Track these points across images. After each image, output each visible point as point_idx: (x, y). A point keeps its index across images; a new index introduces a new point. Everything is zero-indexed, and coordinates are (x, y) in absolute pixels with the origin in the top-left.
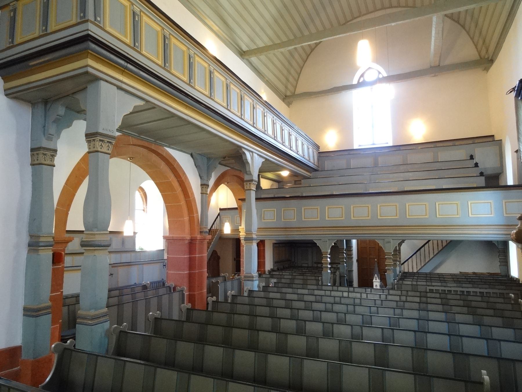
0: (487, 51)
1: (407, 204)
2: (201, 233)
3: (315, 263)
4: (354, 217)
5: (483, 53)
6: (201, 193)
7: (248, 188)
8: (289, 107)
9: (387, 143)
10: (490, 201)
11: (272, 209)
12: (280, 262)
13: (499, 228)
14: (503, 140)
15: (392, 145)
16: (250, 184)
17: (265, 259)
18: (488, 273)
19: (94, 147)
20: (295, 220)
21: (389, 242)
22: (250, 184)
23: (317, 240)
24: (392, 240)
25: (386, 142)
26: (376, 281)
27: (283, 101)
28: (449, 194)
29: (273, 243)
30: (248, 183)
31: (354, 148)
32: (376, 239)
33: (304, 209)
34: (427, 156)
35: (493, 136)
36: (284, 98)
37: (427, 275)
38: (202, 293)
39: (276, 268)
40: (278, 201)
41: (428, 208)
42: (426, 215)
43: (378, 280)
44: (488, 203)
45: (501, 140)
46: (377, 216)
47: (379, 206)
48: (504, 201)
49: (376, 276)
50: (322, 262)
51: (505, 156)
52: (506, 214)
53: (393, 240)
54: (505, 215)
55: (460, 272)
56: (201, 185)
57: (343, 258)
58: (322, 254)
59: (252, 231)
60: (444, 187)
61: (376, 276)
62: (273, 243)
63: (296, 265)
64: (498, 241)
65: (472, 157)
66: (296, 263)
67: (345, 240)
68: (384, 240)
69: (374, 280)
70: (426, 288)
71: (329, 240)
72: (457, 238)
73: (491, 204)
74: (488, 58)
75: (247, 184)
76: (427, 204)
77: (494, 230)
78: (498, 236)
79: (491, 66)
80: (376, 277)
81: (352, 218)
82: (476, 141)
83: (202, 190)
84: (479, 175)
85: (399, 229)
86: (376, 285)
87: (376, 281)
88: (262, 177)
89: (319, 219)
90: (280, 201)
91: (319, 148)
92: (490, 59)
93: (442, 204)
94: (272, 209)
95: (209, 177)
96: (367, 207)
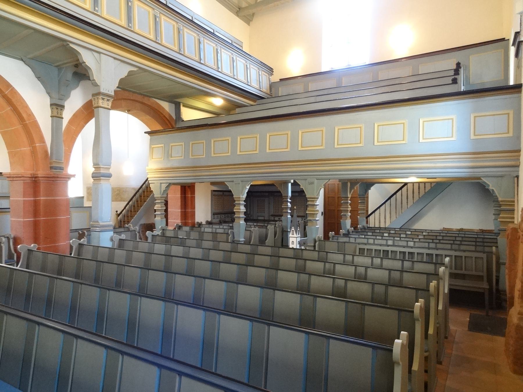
1: (336, 128)
2: (51, 169)
3: (272, 215)
6: (51, 117)
8: (249, 24)
12: (224, 214)
13: (466, 158)
16: (97, 98)
17: (194, 208)
18: (481, 230)
20: (204, 156)
21: (312, 183)
23: (228, 182)
24: (316, 181)
27: (238, 16)
29: (211, 190)
31: (322, 71)
32: (297, 180)
36: (238, 11)
37: (395, 231)
38: (55, 246)
39: (216, 221)
41: (363, 133)
42: (360, 143)
44: (448, 119)
49: (293, 227)
50: (234, 210)
51: (510, 60)
52: (475, 135)
53: (317, 179)
54: (473, 137)
56: (51, 105)
57: (287, 208)
58: (235, 201)
59: (99, 165)
61: (294, 229)
62: (211, 190)
63: (251, 218)
66: (251, 215)
69: (291, 235)
70: (356, 246)
71: (242, 181)
73: (453, 121)
76: (363, 126)
80: (293, 230)
81: (268, 151)
83: (52, 112)
85: (325, 164)
86: (293, 242)
88: (184, 106)
89: (229, 154)
90: (185, 133)
91: (273, 72)
93: (383, 125)
95: (65, 96)
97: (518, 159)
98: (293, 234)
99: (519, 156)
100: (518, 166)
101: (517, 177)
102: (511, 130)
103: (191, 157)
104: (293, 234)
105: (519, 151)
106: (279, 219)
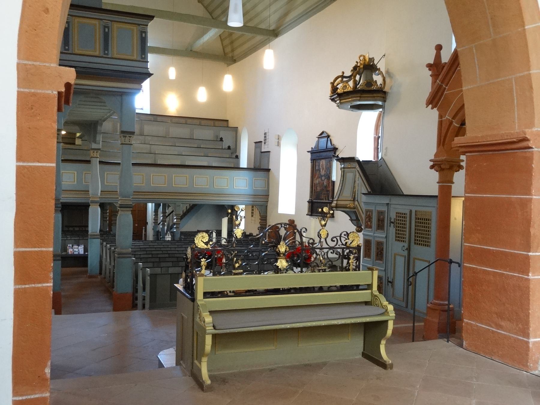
0: (233, 51)
3: (66, 226)
4: (153, 184)
5: (228, 49)
7: (95, 156)
9: (142, 109)
10: (246, 178)
11: (72, 172)
13: (247, 197)
14: (238, 128)
15: (148, 112)
19: (129, 141)
22: (97, 152)
24: (181, 204)
25: (141, 108)
26: (169, 237)
28: (223, 171)
30: (95, 151)
33: (107, 174)
34: (182, 131)
35: (228, 120)
40: (70, 164)
42: (207, 186)
43: (170, 236)
45: (237, 127)
46: (172, 185)
47: (173, 176)
48: (254, 179)
52: (255, 187)
54: (254, 188)
55: (198, 230)
60: (213, 165)
64: (228, 205)
65: (221, 140)
67: (162, 204)
68: (175, 204)
72: (207, 203)
74: (233, 57)
75: (94, 152)
77: (244, 198)
78: (247, 202)
79: (233, 64)
80: (169, 234)
81: (152, 185)
82: (217, 123)
84: (235, 157)
87: (169, 237)
92: (234, 59)
94: (72, 172)
96: (164, 177)
97: (268, 199)
98: (169, 236)
99: (268, 198)
100: (268, 202)
101: (267, 206)
102: (266, 187)
103: (84, 183)
104: (169, 236)
105: (268, 195)
106: (74, 229)
